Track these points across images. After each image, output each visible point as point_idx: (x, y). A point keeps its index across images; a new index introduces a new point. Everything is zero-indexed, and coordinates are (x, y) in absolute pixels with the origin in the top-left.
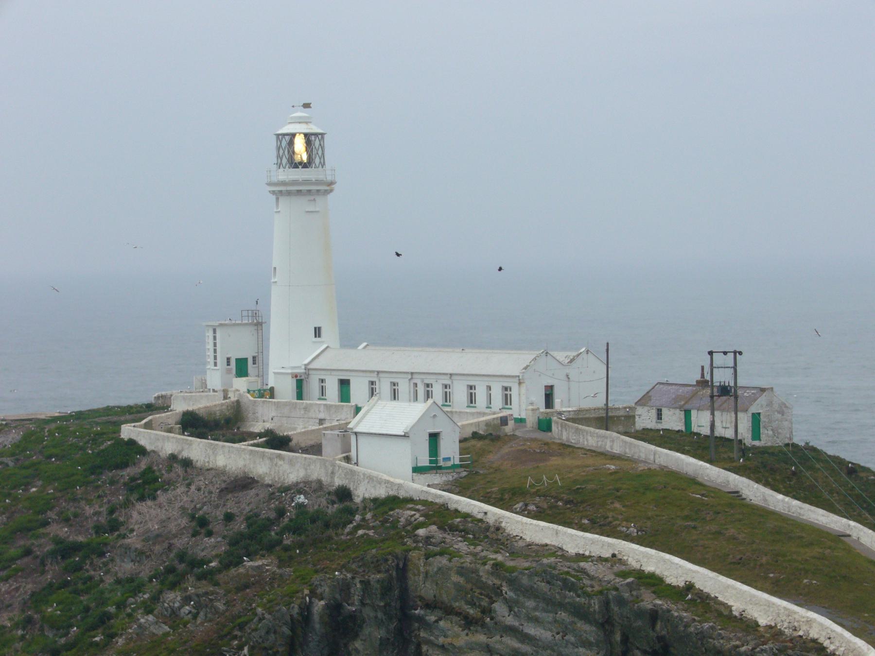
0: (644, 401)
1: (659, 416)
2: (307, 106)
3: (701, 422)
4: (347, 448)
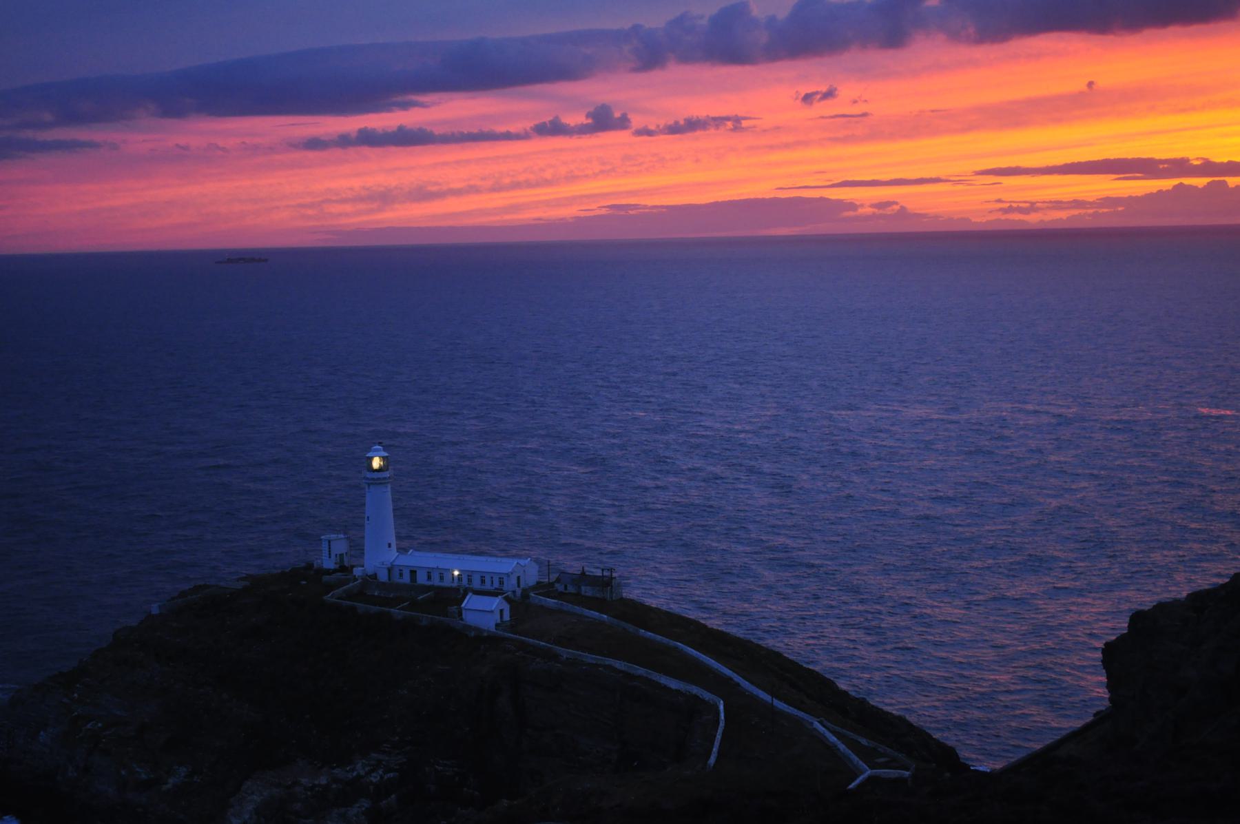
0: (558, 580)
1: (566, 588)
2: (380, 444)
3: (587, 591)
4: (460, 614)
